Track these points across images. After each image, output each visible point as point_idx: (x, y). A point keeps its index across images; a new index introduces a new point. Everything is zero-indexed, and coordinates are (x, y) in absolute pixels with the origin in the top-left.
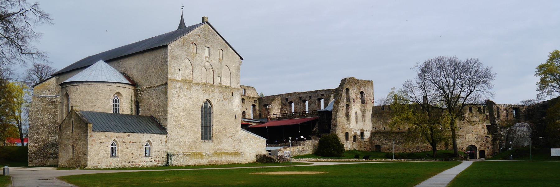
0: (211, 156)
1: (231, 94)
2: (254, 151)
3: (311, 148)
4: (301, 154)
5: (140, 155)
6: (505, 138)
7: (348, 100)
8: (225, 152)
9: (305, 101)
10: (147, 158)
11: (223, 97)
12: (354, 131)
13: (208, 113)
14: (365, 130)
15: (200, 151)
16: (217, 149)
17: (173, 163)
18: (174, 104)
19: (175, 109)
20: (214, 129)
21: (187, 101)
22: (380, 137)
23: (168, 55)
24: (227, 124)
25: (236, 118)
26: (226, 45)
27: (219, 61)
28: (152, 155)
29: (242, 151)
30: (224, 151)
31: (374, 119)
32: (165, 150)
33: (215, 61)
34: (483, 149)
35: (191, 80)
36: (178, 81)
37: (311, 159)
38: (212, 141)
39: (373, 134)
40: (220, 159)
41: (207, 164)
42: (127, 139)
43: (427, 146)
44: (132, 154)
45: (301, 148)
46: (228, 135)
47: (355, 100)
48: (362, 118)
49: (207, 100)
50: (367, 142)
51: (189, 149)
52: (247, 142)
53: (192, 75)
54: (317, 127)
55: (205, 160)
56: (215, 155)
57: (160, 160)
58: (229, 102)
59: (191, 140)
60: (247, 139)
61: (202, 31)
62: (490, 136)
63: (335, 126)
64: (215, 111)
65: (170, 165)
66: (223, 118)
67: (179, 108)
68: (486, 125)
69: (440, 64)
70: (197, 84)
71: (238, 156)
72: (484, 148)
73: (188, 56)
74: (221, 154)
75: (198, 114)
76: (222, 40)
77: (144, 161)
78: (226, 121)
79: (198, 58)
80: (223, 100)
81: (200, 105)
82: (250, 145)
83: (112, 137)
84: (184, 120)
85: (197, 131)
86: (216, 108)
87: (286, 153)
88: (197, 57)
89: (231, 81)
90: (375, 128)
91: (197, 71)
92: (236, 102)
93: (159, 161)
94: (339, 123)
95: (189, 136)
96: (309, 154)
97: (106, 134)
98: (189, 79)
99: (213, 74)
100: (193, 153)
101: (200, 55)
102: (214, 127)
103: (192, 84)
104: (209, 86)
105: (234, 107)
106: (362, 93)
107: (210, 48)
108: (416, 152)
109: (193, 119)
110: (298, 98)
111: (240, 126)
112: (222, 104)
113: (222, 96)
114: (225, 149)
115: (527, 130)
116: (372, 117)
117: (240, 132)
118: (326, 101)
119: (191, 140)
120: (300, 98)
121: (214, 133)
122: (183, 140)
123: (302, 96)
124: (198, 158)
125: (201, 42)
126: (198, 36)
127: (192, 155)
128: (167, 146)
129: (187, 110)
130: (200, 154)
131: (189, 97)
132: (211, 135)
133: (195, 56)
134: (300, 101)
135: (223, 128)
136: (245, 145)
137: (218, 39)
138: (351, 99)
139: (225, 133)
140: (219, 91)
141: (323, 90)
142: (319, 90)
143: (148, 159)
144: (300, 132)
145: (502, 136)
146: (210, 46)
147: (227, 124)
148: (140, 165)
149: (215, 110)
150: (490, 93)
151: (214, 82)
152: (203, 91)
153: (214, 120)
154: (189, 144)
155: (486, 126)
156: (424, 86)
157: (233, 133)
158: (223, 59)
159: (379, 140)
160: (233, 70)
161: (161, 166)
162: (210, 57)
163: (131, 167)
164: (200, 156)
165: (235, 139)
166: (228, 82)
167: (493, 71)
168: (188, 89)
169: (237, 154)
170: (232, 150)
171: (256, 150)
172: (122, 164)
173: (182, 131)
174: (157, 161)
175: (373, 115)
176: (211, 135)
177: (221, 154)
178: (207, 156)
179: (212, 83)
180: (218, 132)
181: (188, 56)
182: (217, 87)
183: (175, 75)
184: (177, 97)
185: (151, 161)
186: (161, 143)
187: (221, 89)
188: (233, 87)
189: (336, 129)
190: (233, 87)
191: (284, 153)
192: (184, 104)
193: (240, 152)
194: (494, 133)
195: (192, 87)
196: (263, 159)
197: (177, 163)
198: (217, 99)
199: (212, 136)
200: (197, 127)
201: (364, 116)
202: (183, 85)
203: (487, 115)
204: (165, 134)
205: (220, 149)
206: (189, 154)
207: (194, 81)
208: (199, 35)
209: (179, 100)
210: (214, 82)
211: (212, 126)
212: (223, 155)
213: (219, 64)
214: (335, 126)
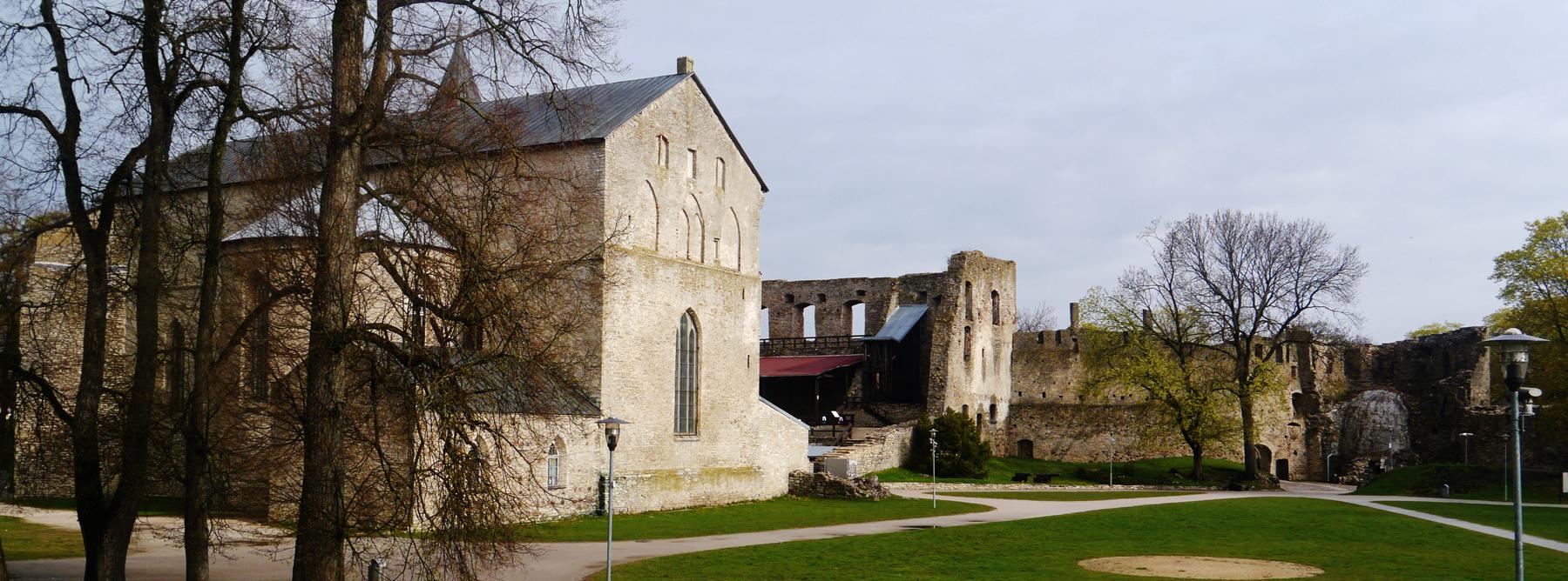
1: (740, 293)
3: (896, 451)
6: (1337, 429)
7: (969, 317)
9: (801, 307)
12: (979, 402)
14: (998, 397)
15: (671, 468)
19: (619, 337)
20: (701, 397)
21: (645, 313)
22: (1031, 418)
23: (606, 169)
28: (565, 481)
31: (1018, 367)
34: (1284, 455)
35: (654, 248)
37: (916, 483)
38: (696, 434)
39: (1014, 408)
40: (717, 489)
41: (689, 505)
43: (1183, 451)
45: (877, 451)
46: (733, 416)
47: (982, 314)
48: (993, 366)
49: (689, 311)
50: (1001, 432)
53: (658, 233)
54: (860, 386)
61: (680, 99)
62: (1301, 422)
63: (943, 388)
67: (627, 334)
68: (1292, 393)
69: (1228, 230)
70: (668, 262)
72: (1287, 453)
73: (649, 175)
75: (669, 352)
79: (670, 182)
82: (777, 445)
85: (665, 405)
89: (739, 255)
90: (1020, 394)
94: (952, 380)
95: (649, 422)
96: (893, 468)
99: (700, 232)
100: (656, 471)
101: (677, 174)
102: (703, 391)
103: (656, 262)
104: (693, 269)
106: (994, 294)
107: (698, 154)
108: (1122, 461)
110: (783, 297)
113: (722, 298)
115: (1397, 410)
116: (1012, 362)
118: (873, 311)
120: (790, 298)
121: (702, 410)
123: (795, 291)
124: (669, 489)
128: (599, 452)
131: (650, 302)
132: (694, 418)
134: (788, 306)
138: (975, 313)
141: (863, 279)
142: (853, 279)
144: (818, 397)
145: (1330, 422)
146: (700, 147)
148: (536, 514)
150: (1352, 315)
151: (702, 256)
153: (704, 372)
154: (646, 444)
155: (1293, 394)
156: (1170, 285)
157: (742, 412)
158: (723, 188)
159: (1030, 426)
160: (745, 224)
161: (585, 516)
162: (698, 180)
164: (673, 481)
165: (745, 428)
167: (1362, 257)
169: (751, 472)
170: (738, 463)
171: (789, 458)
175: (1014, 360)
176: (694, 418)
177: (714, 473)
179: (735, 266)
180: (711, 408)
182: (713, 271)
189: (944, 396)
190: (743, 272)
194: (1310, 416)
195: (657, 269)
196: (812, 487)
197: (623, 504)
199: (697, 421)
201: (996, 358)
202: (639, 263)
203: (1293, 367)
204: (593, 416)
205: (715, 460)
207: (662, 253)
210: (702, 256)
211: (697, 388)
212: (723, 477)
214: (943, 387)
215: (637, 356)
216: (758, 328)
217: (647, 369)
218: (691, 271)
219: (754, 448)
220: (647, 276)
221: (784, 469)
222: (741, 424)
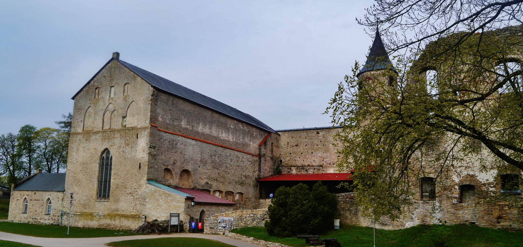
0: (102, 217)
1: (135, 137)
2: (164, 215)
4: (259, 225)
5: (41, 212)
8: (123, 213)
10: (46, 216)
11: (125, 142)
12: (465, 173)
13: (105, 164)
16: (113, 210)
17: (63, 223)
18: (73, 159)
19: (74, 164)
21: (85, 153)
24: (127, 176)
25: (140, 168)
26: (134, 76)
27: (124, 99)
29: (146, 213)
30: (121, 212)
32: (61, 208)
33: (119, 101)
36: (79, 134)
40: (113, 222)
42: (34, 197)
44: (36, 211)
51: (83, 208)
52: (154, 200)
55: (94, 222)
56: (107, 217)
57: (56, 219)
58: (131, 148)
59: (85, 198)
60: (154, 196)
64: (114, 161)
65: (60, 225)
66: (123, 169)
67: (77, 162)
70: (97, 133)
71: (137, 220)
74: (115, 216)
75: (95, 167)
76: (130, 71)
77: (44, 219)
78: (127, 172)
80: (125, 146)
81: (97, 156)
83: (24, 195)
84: (80, 176)
86: (115, 157)
87: (224, 221)
88: (100, 102)
91: (98, 117)
92: (141, 146)
93: (55, 220)
97: (21, 192)
98: (91, 129)
100: (85, 212)
103: (91, 134)
104: (109, 132)
109: (89, 173)
111: (145, 178)
112: (123, 151)
114: (123, 209)
117: (145, 186)
119: (85, 198)
125: (106, 84)
126: (103, 78)
127: (82, 215)
129: (84, 164)
130: (91, 214)
133: (98, 102)
135: (123, 183)
136: (150, 205)
137: (125, 72)
139: (124, 189)
140: (121, 135)
143: (47, 217)
147: (127, 176)
149: (113, 158)
152: (102, 139)
153: (113, 172)
154: (82, 202)
157: (135, 189)
163: (34, 223)
164: (90, 217)
166: (134, 122)
168: (87, 140)
172: (28, 219)
173: (78, 188)
174: (53, 220)
178: (98, 218)
181: (90, 104)
183: (78, 128)
185: (49, 220)
186: (58, 201)
187: (124, 133)
188: (139, 127)
191: (219, 221)
193: (141, 216)
200: (93, 183)
202: (83, 137)
205: (117, 210)
206: (80, 213)
208: (105, 76)
209: (78, 153)
212: (117, 218)
213: (124, 102)
215: (81, 169)
216: (146, 150)
217: (85, 174)
218: (108, 133)
219: (142, 206)
220: (87, 140)
221: (164, 218)
222: (134, 194)
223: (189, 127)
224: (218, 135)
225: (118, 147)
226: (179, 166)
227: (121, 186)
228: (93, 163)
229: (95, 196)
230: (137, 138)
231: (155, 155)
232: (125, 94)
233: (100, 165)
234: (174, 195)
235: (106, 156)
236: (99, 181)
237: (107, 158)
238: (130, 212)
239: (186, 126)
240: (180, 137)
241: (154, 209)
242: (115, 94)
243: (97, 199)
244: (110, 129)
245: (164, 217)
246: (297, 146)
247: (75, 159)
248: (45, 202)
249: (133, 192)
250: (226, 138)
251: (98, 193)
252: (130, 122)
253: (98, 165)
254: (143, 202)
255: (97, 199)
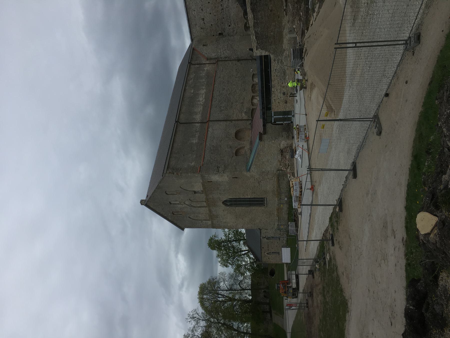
8: (276, 187)
11: (215, 190)
13: (236, 203)
25: (237, 178)
30: (275, 188)
44: (277, 246)
57: (282, 233)
58: (220, 185)
70: (210, 211)
75: (239, 209)
81: (229, 209)
86: (229, 196)
93: (283, 233)
104: (209, 202)
105: (225, 180)
112: (224, 191)
122: (265, 219)
135: (250, 189)
149: (230, 198)
153: (242, 197)
157: (255, 180)
183: (208, 224)
184: (227, 223)
192: (231, 219)
198: (219, 195)
206: (277, 217)
215: (241, 219)
219: (269, 174)
220: (217, 217)
223: (197, 135)
224: (201, 105)
225: (220, 195)
226: (232, 142)
227: (253, 190)
228: (235, 211)
229: (263, 208)
230: (211, 181)
231: (225, 166)
232: (175, 193)
233: (237, 206)
234: (258, 150)
235: (229, 202)
236: (250, 206)
237: (230, 201)
238: (274, 182)
239: (197, 138)
240: (206, 143)
241: (271, 165)
242: (176, 201)
243: (265, 206)
244: (206, 201)
245: (277, 157)
246: (203, 19)
247: (234, 224)
248: (269, 241)
249: (258, 181)
250: (204, 96)
251: (260, 206)
252: (198, 187)
253: (237, 208)
254: (266, 173)
255: (265, 206)
